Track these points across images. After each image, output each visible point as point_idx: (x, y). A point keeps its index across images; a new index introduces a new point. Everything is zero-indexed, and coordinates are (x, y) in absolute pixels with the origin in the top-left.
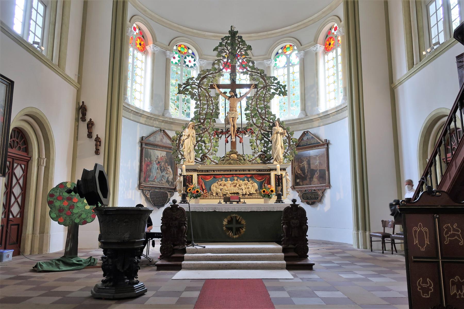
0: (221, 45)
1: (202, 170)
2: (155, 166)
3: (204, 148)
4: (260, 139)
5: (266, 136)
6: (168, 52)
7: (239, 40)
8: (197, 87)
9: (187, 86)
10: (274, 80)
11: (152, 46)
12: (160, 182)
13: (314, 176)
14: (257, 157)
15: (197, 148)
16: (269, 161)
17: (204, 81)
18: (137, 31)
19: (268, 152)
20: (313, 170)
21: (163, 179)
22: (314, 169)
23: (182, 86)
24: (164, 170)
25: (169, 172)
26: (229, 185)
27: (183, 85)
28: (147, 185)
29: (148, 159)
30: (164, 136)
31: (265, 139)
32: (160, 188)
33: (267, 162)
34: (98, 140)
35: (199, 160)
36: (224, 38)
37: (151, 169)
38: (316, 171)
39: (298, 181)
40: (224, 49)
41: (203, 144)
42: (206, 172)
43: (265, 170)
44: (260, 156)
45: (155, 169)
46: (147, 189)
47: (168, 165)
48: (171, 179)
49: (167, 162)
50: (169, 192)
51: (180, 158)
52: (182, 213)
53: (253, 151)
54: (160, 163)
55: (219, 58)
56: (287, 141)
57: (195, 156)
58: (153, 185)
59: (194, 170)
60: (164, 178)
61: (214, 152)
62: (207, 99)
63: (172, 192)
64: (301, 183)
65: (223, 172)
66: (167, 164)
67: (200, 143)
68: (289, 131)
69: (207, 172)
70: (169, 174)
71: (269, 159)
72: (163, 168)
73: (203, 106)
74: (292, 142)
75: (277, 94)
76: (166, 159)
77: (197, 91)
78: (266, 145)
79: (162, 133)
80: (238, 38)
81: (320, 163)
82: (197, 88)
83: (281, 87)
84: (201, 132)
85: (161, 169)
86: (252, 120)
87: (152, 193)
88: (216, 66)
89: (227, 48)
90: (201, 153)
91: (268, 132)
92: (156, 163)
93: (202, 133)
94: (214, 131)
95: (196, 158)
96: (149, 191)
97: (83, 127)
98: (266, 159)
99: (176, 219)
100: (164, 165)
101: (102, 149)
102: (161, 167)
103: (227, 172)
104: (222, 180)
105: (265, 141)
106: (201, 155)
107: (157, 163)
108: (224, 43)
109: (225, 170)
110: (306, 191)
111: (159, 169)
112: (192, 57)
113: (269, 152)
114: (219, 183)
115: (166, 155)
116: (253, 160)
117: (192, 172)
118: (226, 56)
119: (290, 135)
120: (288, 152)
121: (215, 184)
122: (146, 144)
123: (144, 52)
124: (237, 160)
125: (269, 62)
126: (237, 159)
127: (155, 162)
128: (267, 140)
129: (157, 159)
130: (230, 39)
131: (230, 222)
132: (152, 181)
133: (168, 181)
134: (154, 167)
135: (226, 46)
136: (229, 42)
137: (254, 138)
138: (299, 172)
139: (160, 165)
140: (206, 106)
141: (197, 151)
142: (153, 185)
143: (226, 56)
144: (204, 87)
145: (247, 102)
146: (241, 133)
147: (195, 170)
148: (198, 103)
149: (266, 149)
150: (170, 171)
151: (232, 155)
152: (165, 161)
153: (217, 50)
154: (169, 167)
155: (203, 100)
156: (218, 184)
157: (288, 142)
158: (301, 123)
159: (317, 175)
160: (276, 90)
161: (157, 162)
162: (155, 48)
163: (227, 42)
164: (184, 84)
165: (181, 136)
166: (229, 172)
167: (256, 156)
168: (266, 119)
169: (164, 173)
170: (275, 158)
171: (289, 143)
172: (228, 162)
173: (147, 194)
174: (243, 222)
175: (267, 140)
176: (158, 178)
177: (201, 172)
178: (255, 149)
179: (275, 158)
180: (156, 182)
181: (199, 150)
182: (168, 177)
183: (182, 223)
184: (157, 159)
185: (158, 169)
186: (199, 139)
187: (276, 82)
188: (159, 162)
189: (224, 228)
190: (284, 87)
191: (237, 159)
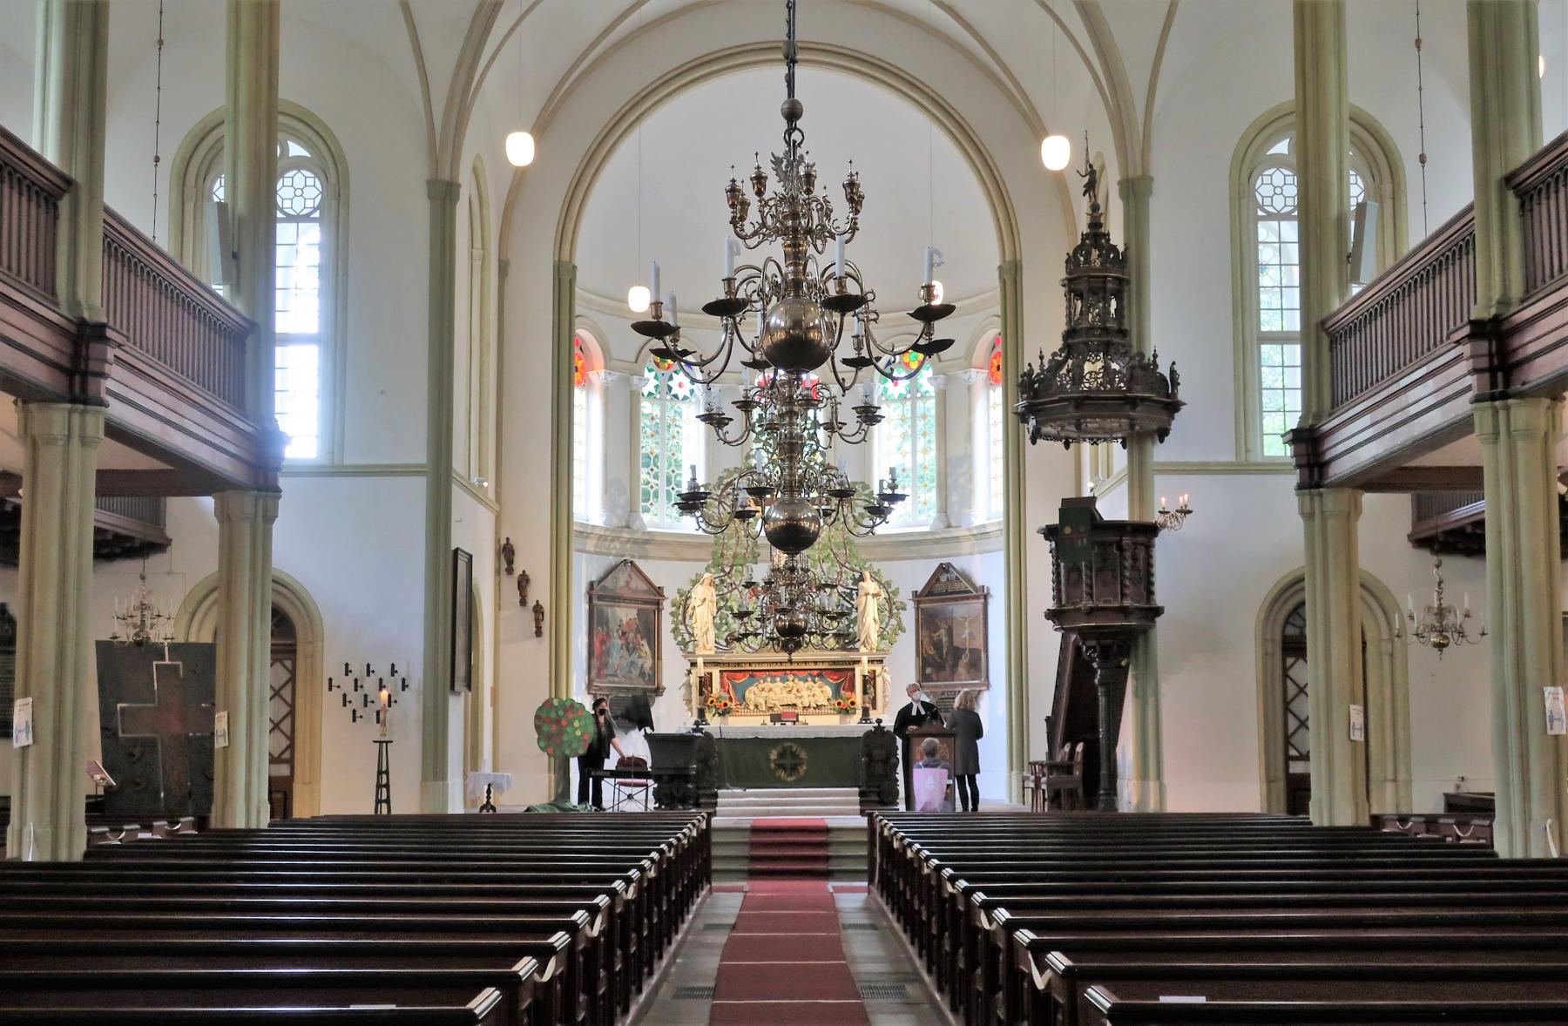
2: (617, 642)
6: (635, 379)
10: (863, 489)
13: (960, 663)
15: (718, 621)
20: (958, 648)
22: (960, 646)
24: (634, 649)
26: (778, 690)
30: (632, 574)
34: (538, 609)
38: (964, 650)
39: (928, 671)
47: (642, 639)
49: (639, 632)
51: (687, 640)
56: (887, 607)
64: (934, 677)
66: (639, 636)
67: (723, 611)
71: (853, 641)
72: (631, 645)
81: (971, 634)
84: (726, 590)
85: (628, 649)
91: (852, 589)
97: (510, 584)
101: (546, 625)
102: (628, 643)
104: (765, 681)
106: (727, 633)
110: (943, 693)
121: (753, 688)
122: (601, 598)
127: (616, 634)
128: (850, 606)
131: (781, 755)
133: (642, 674)
138: (930, 652)
141: (717, 627)
142: (614, 682)
147: (716, 664)
154: (644, 642)
158: (937, 541)
159: (964, 660)
165: (687, 598)
168: (847, 565)
169: (634, 657)
170: (862, 640)
171: (890, 611)
174: (803, 755)
175: (850, 606)
179: (862, 640)
182: (642, 665)
186: (722, 604)
187: (867, 492)
188: (624, 634)
189: (772, 766)
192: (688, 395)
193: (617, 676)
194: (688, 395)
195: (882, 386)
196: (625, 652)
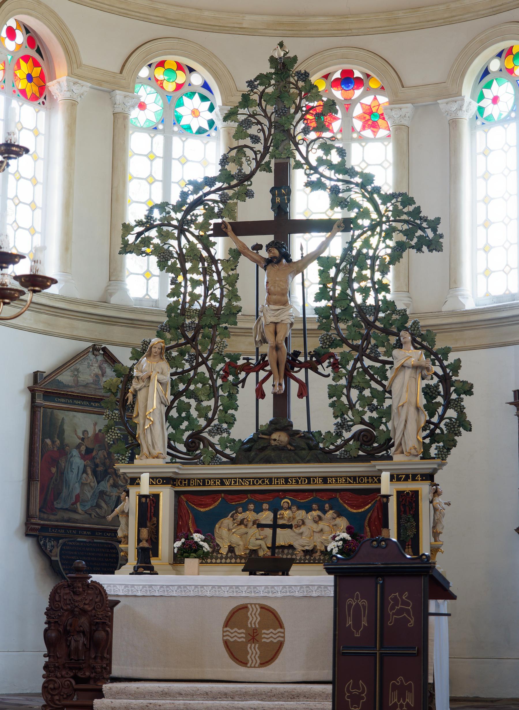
0: (246, 101)
1: (189, 480)
2: (78, 462)
3: (194, 413)
4: (357, 384)
5: (376, 376)
6: (119, 95)
7: (301, 84)
8: (176, 232)
9: (147, 229)
11: (64, 84)
12: (94, 514)
14: (349, 440)
15: (174, 413)
16: (385, 452)
17: (195, 212)
18: (20, 37)
19: (382, 423)
21: (103, 504)
23: (132, 228)
25: (124, 481)
27: (136, 226)
28: (50, 520)
29: (53, 442)
30: (105, 365)
31: (373, 384)
32: (93, 531)
33: (380, 454)
35: (182, 447)
36: (256, 80)
37: (62, 473)
40: (256, 114)
41: (193, 402)
42: (199, 485)
43: (372, 477)
44: (356, 437)
45: (75, 471)
46: (51, 534)
52: (97, 597)
53: (339, 420)
54: (94, 453)
55: (242, 142)
56: (441, 389)
57: (169, 439)
58: (68, 521)
59: (163, 479)
60: (104, 501)
61: (225, 426)
62: (204, 269)
65: (249, 485)
67: (183, 398)
68: (447, 360)
69: (204, 485)
72: (100, 469)
73: (194, 287)
74: (455, 390)
75: (413, 247)
77: (175, 243)
78: (375, 402)
79: (100, 358)
80: (296, 78)
82: (176, 235)
83: (425, 225)
84: (187, 366)
85: (95, 473)
86: (337, 328)
87: (68, 548)
88: (233, 168)
89: (264, 111)
90: (187, 429)
92: (81, 454)
93: (189, 370)
94: (224, 361)
95: (172, 442)
96: (57, 539)
98: (375, 445)
99: (84, 612)
100: (106, 459)
102: (97, 466)
103: (260, 484)
105: (373, 390)
106: (187, 434)
107: (83, 452)
108: (256, 97)
109: (255, 478)
111: (89, 471)
112: (204, 98)
113: (385, 424)
114: (240, 517)
116: (338, 448)
117: (157, 484)
118: (261, 135)
119: (448, 370)
120: (444, 422)
121: (227, 521)
122: (48, 395)
123: (42, 99)
124: (290, 450)
125: (454, 107)
126: (289, 447)
127: (75, 452)
129: (83, 439)
130: (273, 82)
134: (71, 465)
135: (260, 105)
136: (270, 90)
137: (343, 382)
139: (94, 458)
140: (200, 290)
141: (175, 423)
142: (68, 521)
143: (261, 135)
144: (196, 233)
145: (323, 274)
146: (303, 370)
148: (180, 279)
149: (375, 415)
151: (275, 436)
153: (233, 118)
155: (194, 270)
156: (234, 520)
157: (442, 393)
160: (410, 234)
161: (83, 448)
162: (75, 88)
163: (264, 91)
164: (140, 223)
166: (267, 484)
167: (347, 435)
168: (378, 324)
171: (447, 396)
172: (262, 455)
173: (51, 551)
175: (380, 389)
177: (185, 484)
178: (343, 414)
180: (80, 511)
181: (180, 420)
183: (97, 622)
184: (83, 439)
185: (85, 471)
186: (182, 387)
188: (89, 451)
190: (434, 224)
191: (289, 447)
192: (206, 127)
193: (75, 511)
194: (206, 127)
195: (475, 105)
196: (90, 478)
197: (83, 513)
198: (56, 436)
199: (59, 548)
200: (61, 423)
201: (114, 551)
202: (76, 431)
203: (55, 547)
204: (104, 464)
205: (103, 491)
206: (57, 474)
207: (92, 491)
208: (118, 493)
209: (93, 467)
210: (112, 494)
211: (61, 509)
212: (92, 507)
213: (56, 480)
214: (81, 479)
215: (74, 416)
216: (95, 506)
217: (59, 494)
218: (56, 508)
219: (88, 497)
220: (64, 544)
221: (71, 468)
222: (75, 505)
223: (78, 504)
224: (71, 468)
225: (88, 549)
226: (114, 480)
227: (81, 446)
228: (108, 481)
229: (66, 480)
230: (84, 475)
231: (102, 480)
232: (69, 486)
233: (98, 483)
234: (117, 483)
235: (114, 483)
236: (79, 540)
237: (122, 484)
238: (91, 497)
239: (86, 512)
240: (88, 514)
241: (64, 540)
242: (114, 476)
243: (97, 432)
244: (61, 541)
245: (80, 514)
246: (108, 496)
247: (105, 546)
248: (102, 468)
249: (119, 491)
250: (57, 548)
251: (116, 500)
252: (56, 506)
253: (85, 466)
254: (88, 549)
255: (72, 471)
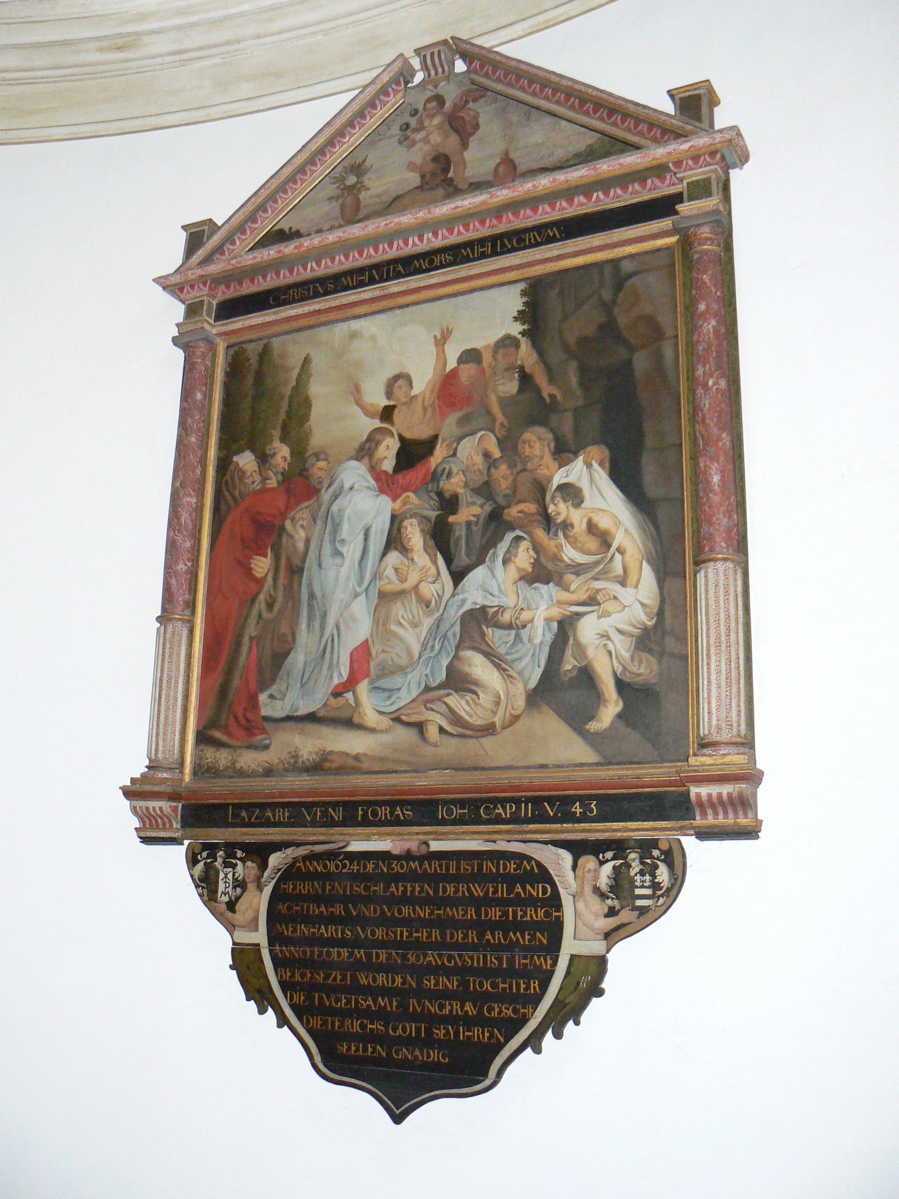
12: (436, 719)
25: (592, 544)
29: (263, 459)
37: (296, 571)
45: (352, 550)
48: (622, 647)
50: (578, 849)
60: (490, 655)
63: (646, 846)
70: (578, 570)
76: (525, 379)
102: (449, 504)
107: (388, 465)
111: (415, 536)
115: (516, 329)
129: (387, 414)
132: (312, 718)
134: (336, 527)
150: (604, 523)
152: (505, 403)
176: (402, 670)
180: (371, 717)
197: (385, 722)
198: (276, 433)
199: (268, 890)
200: (298, 381)
201: (537, 891)
202: (357, 389)
203: (251, 887)
204: (485, 490)
205: (484, 608)
206: (275, 579)
207: (427, 622)
208: (560, 603)
209: (433, 514)
210: (525, 616)
211: (289, 718)
212: (428, 689)
213: (270, 606)
214: (376, 576)
215: (354, 335)
216: (440, 687)
217: (280, 658)
218: (267, 719)
219: (409, 653)
220: (289, 873)
221: (333, 541)
222: (349, 696)
223: (363, 688)
224: (333, 541)
225: (397, 889)
226: (537, 547)
227: (378, 443)
228: (505, 562)
229: (312, 596)
230: (394, 557)
231: (480, 561)
232: (324, 616)
233: (458, 577)
234: (556, 558)
235: (536, 563)
236: (356, 846)
237: (581, 558)
238: (424, 646)
239: (397, 720)
240: (408, 724)
241: (291, 853)
242: (540, 533)
243: (452, 364)
244: (275, 860)
245: (373, 730)
246: (509, 626)
247: (489, 866)
248: (476, 510)
249: (565, 596)
250: (260, 888)
251: (549, 637)
252: (265, 712)
253: (396, 520)
254: (397, 889)
255: (338, 554)
